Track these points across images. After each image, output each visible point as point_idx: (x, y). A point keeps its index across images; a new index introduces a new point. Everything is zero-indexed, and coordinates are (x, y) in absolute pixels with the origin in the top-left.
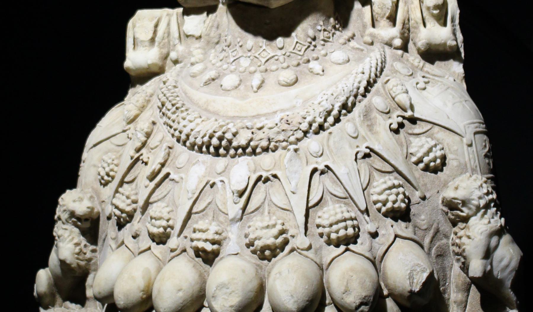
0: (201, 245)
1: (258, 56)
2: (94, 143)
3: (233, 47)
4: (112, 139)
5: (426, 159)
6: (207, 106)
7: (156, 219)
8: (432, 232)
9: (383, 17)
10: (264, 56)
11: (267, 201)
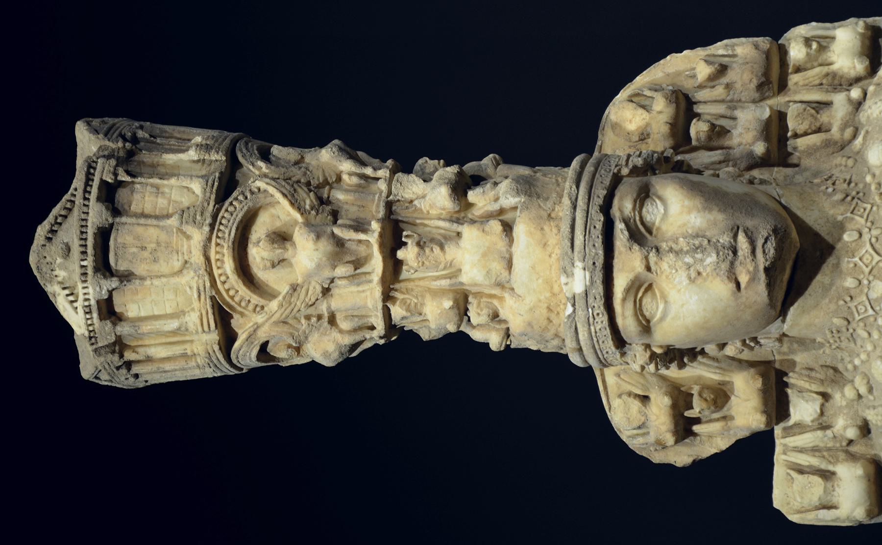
1: (870, 267)
3: (852, 313)
9: (816, 119)
10: (870, 258)
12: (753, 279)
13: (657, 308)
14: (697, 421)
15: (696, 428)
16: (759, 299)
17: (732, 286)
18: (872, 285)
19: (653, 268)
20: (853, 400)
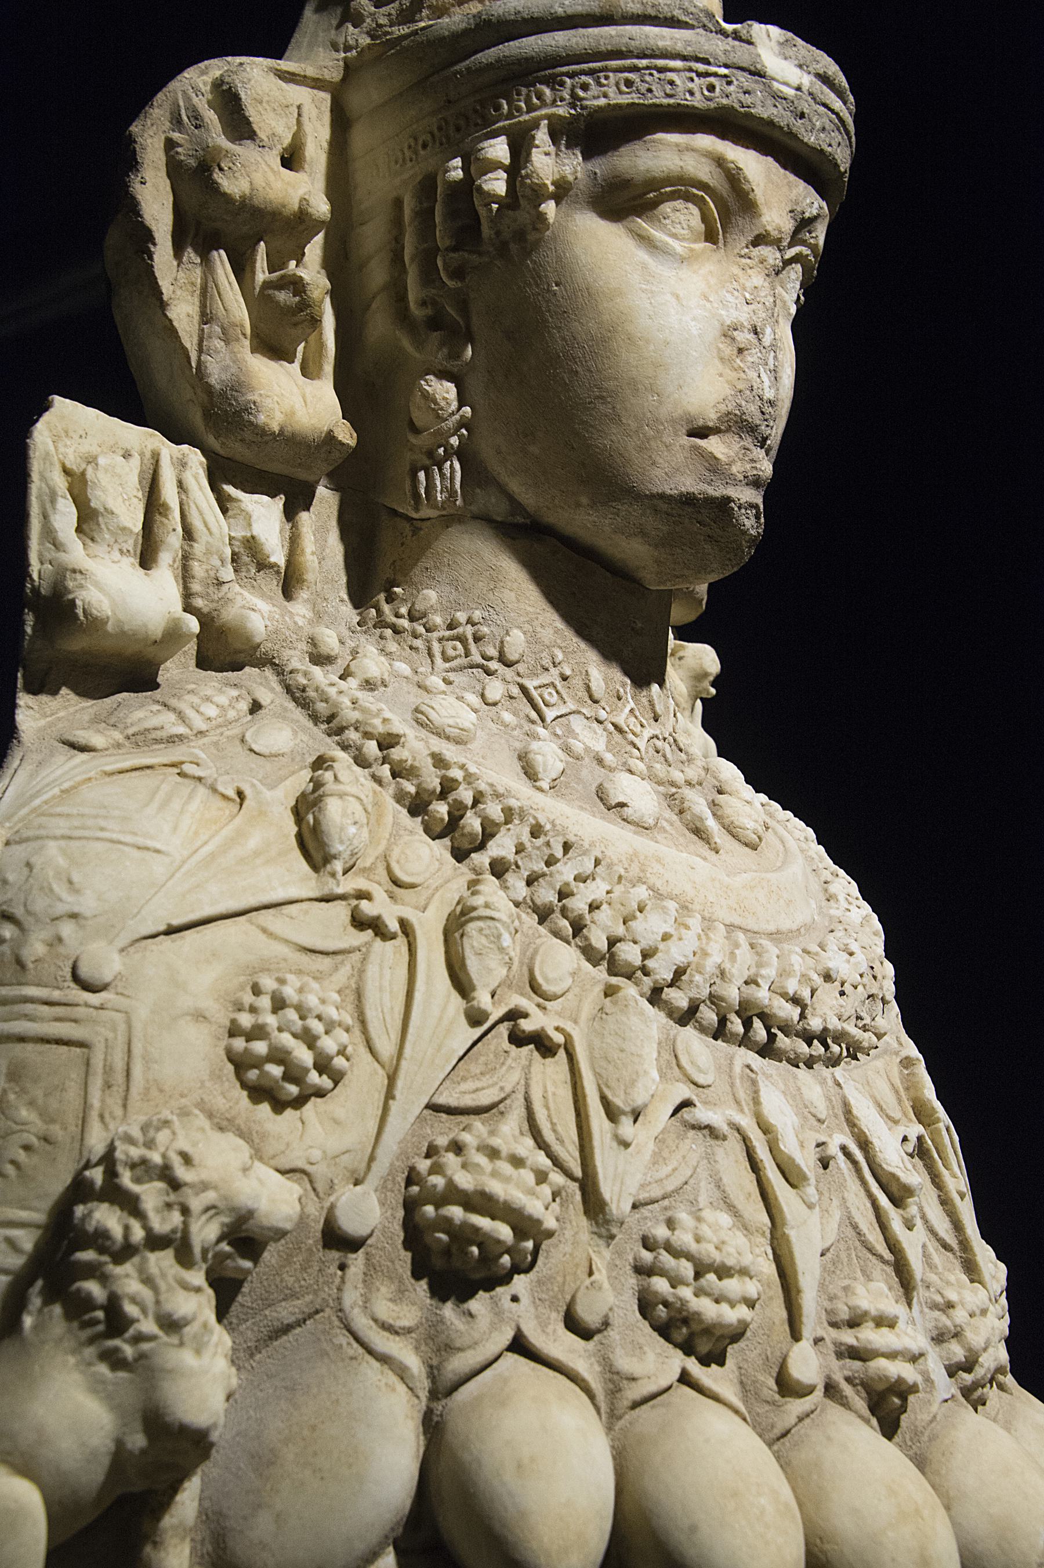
2: (176, 922)
4: (265, 918)
7: (723, 1272)
12: (714, 467)
13: (674, 236)
14: (241, 268)
15: (221, 259)
16: (658, 472)
17: (712, 418)
18: (595, 725)
19: (756, 252)
20: (313, 641)
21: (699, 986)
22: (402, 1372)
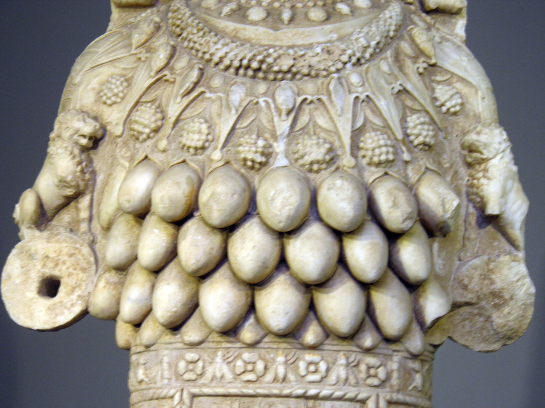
0: (250, 156)
5: (448, 105)
6: (237, 33)
8: (451, 173)
11: (311, 123)
21: (227, 62)
22: (125, 168)
